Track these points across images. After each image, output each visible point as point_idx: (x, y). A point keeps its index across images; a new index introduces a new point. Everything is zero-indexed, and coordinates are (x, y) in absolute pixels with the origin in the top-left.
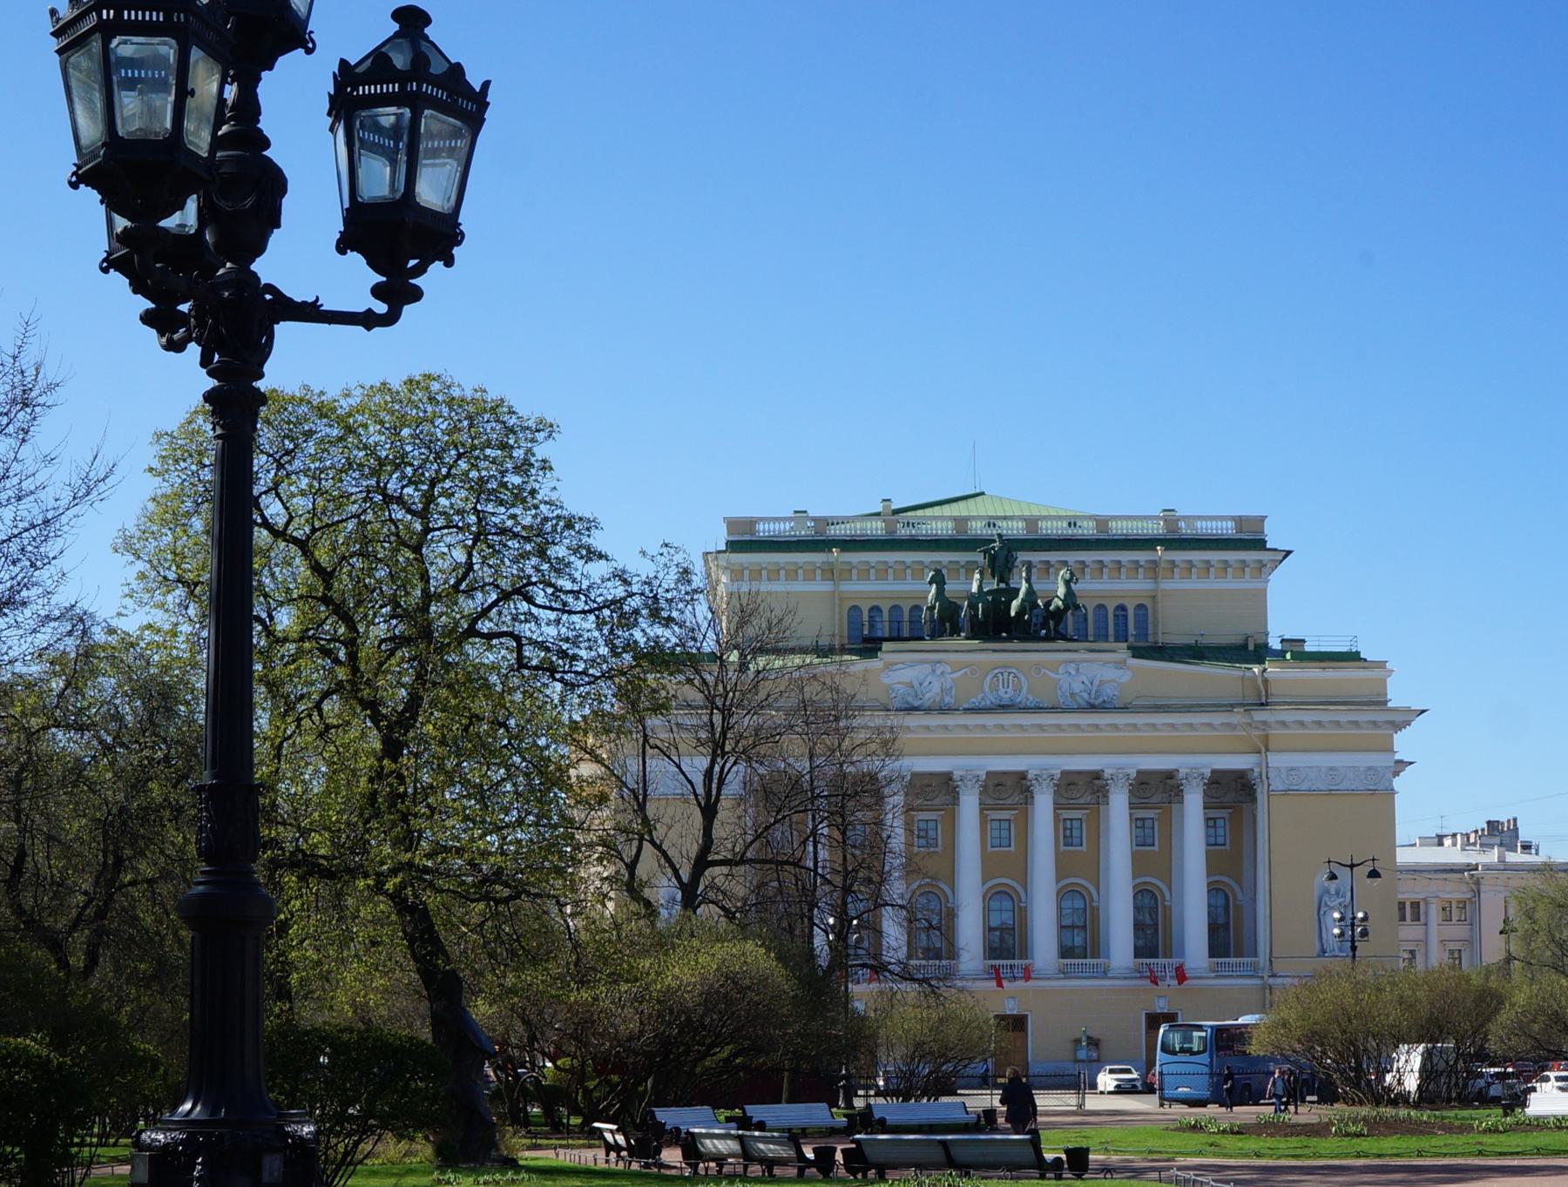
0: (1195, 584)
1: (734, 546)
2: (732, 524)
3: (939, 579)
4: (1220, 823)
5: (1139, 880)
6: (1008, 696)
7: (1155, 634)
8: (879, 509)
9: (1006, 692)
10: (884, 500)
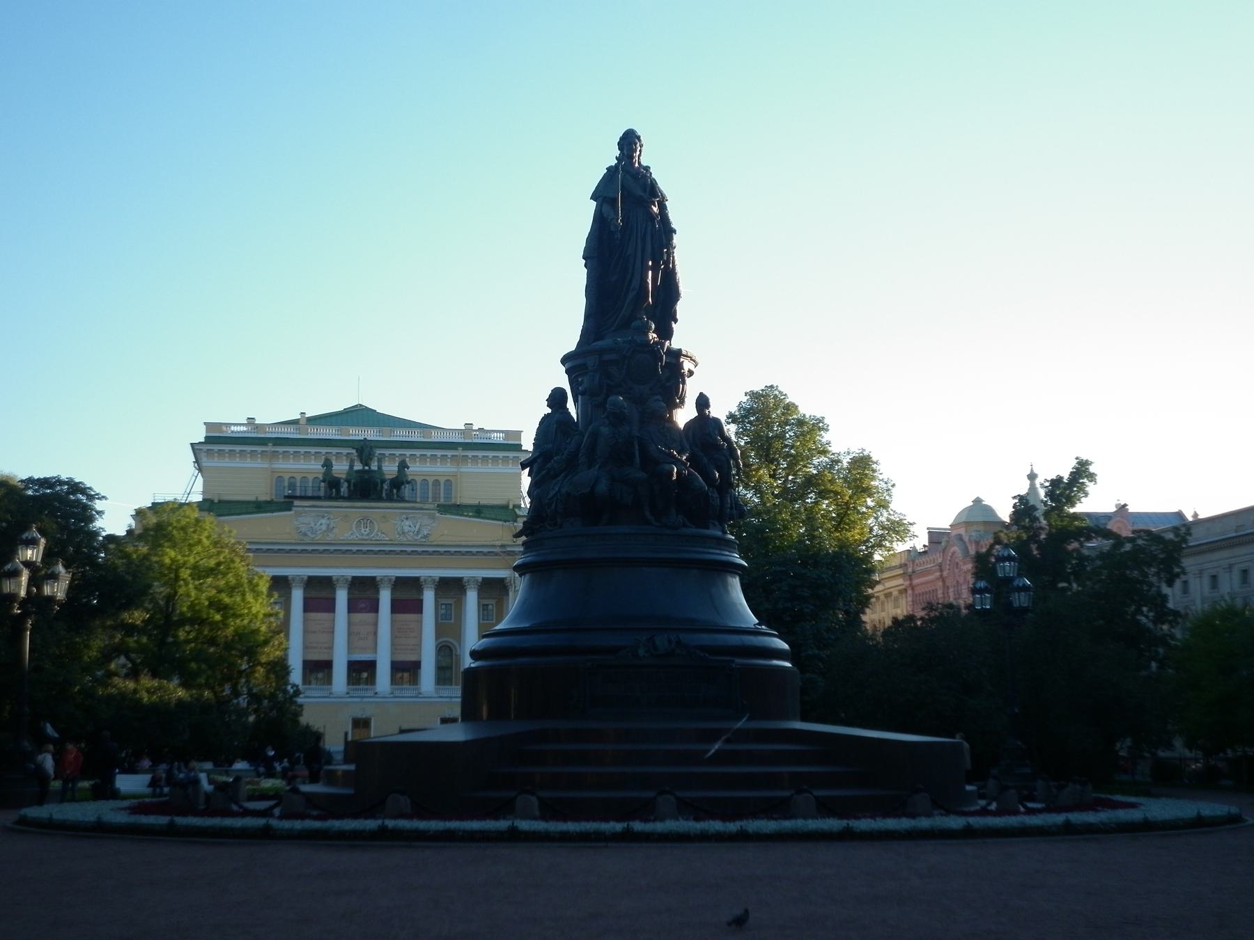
0: (479, 468)
1: (209, 440)
2: (209, 426)
3: (328, 464)
4: (490, 607)
5: (441, 640)
6: (366, 533)
7: (456, 498)
8: (299, 417)
9: (365, 531)
10: (302, 413)
